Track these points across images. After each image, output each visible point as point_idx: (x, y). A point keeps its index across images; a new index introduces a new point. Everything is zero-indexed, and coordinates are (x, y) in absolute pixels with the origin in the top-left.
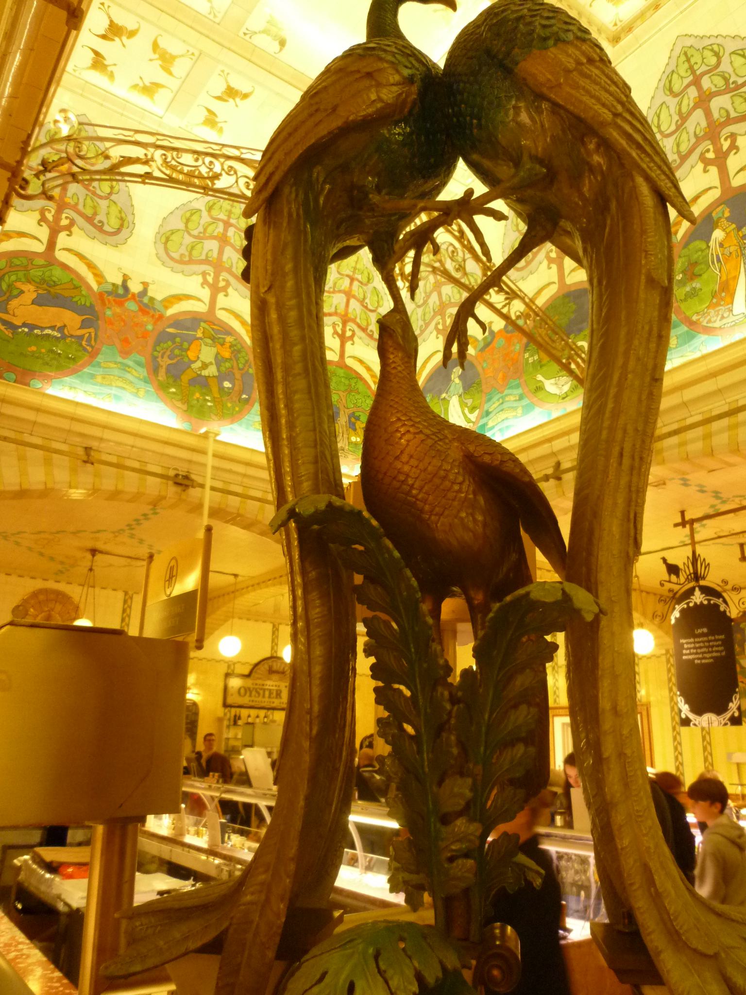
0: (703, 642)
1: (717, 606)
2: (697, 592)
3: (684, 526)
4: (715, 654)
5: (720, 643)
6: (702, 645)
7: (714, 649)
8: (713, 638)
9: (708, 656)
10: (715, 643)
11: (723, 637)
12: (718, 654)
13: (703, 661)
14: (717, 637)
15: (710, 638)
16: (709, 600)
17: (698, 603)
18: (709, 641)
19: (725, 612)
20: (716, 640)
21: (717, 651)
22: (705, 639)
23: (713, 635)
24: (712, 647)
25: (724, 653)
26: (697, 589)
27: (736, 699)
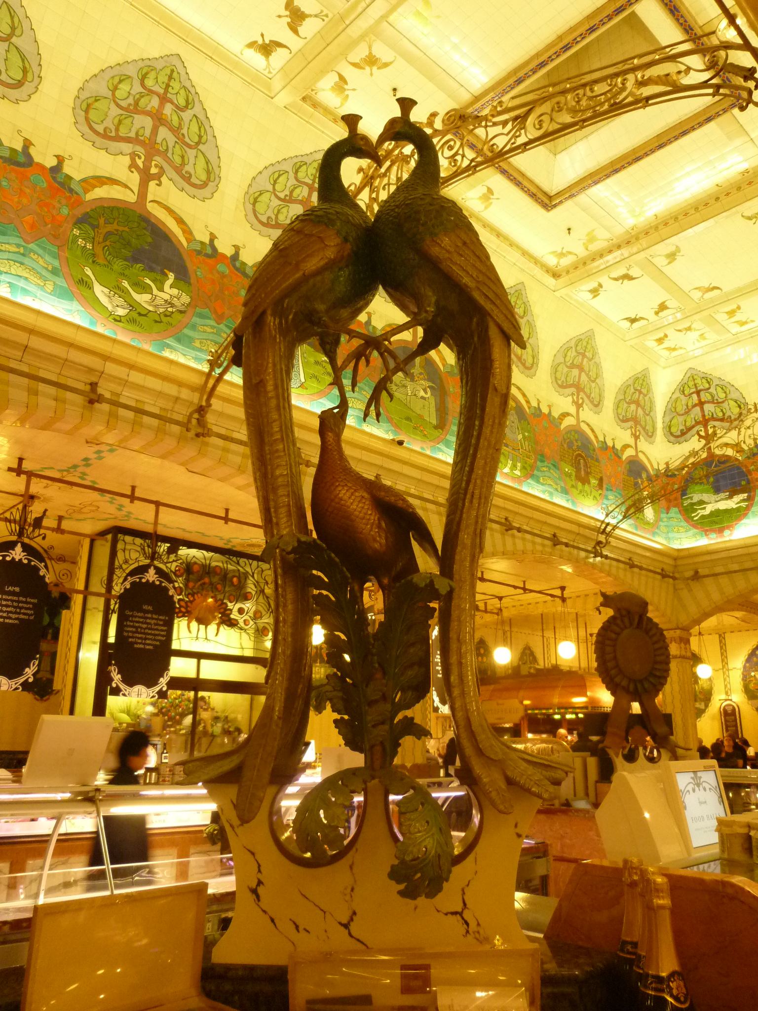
0: (12, 601)
1: (37, 569)
2: (19, 548)
3: (18, 475)
4: (22, 616)
5: (31, 606)
6: (9, 603)
7: (22, 611)
8: (24, 599)
9: (14, 616)
10: (25, 605)
11: (35, 601)
12: (26, 617)
13: (7, 621)
14: (29, 600)
15: (21, 598)
16: (30, 561)
17: (17, 560)
18: (19, 602)
19: (44, 576)
20: (26, 602)
21: (24, 614)
22: (15, 598)
23: (24, 597)
24: (21, 608)
25: (32, 618)
26: (19, 545)
27: (34, 664)
